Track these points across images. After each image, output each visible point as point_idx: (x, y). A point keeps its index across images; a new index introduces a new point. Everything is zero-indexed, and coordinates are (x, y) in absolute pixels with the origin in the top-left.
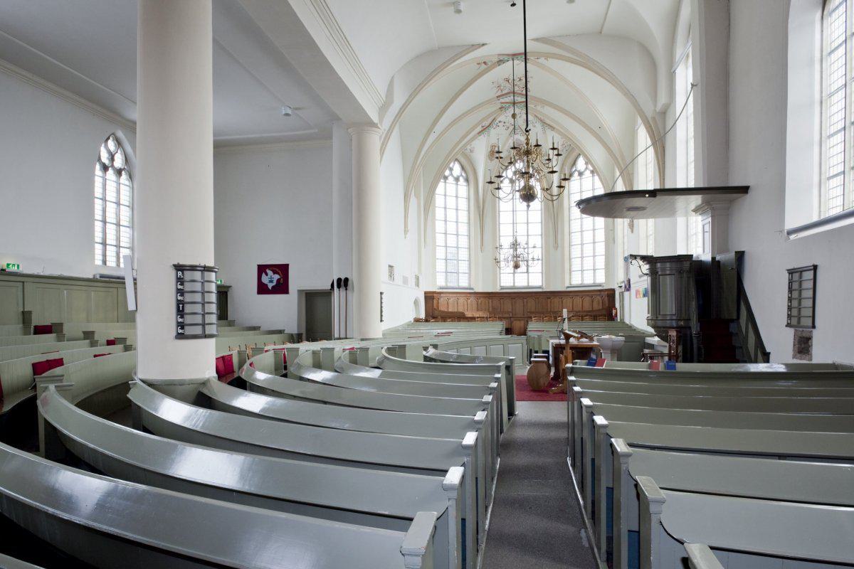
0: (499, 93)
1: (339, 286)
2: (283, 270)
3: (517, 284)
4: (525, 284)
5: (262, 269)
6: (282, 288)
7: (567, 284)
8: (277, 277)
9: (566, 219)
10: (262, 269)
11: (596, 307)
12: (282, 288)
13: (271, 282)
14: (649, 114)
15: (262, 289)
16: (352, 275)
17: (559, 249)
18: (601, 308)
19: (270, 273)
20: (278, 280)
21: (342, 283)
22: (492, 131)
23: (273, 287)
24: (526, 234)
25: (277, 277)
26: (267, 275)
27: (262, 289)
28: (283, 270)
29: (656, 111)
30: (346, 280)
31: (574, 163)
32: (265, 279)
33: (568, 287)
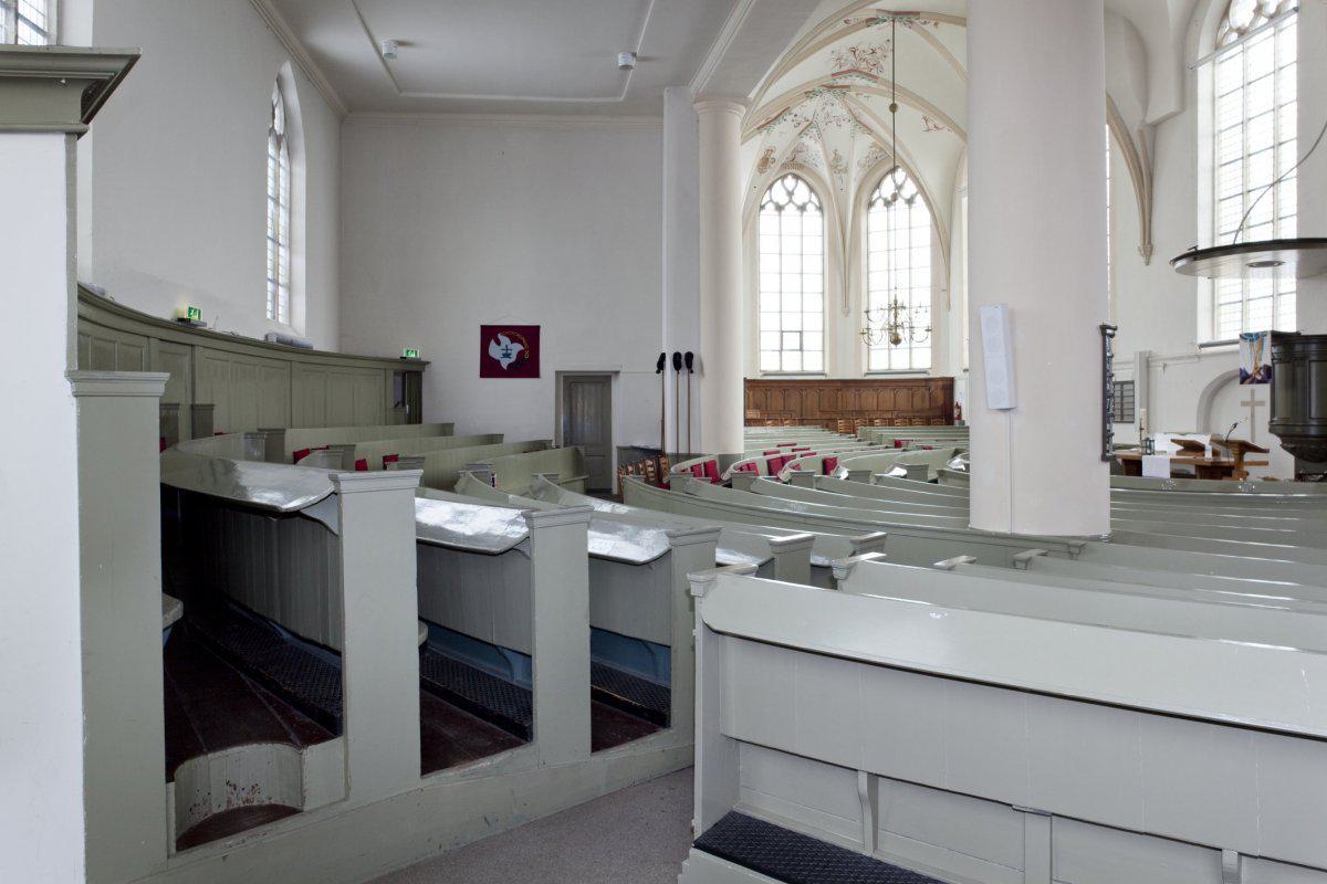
0: (836, 70)
1: (677, 365)
2: (529, 336)
3: (786, 368)
4: (797, 368)
5: (489, 333)
6: (527, 366)
7: (865, 370)
8: (517, 348)
9: (864, 269)
10: (489, 333)
11: (918, 403)
12: (527, 366)
13: (507, 355)
14: (1134, 123)
15: (490, 368)
16: (699, 348)
17: (852, 314)
18: (927, 405)
19: (504, 340)
20: (520, 354)
21: (683, 360)
22: (777, 128)
23: (510, 365)
24: (799, 290)
25: (517, 348)
26: (498, 343)
27: (490, 368)
28: (529, 336)
29: (1144, 120)
30: (689, 356)
31: (878, 186)
32: (495, 351)
33: (867, 374)
